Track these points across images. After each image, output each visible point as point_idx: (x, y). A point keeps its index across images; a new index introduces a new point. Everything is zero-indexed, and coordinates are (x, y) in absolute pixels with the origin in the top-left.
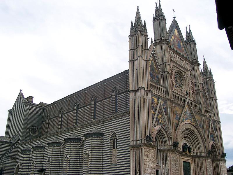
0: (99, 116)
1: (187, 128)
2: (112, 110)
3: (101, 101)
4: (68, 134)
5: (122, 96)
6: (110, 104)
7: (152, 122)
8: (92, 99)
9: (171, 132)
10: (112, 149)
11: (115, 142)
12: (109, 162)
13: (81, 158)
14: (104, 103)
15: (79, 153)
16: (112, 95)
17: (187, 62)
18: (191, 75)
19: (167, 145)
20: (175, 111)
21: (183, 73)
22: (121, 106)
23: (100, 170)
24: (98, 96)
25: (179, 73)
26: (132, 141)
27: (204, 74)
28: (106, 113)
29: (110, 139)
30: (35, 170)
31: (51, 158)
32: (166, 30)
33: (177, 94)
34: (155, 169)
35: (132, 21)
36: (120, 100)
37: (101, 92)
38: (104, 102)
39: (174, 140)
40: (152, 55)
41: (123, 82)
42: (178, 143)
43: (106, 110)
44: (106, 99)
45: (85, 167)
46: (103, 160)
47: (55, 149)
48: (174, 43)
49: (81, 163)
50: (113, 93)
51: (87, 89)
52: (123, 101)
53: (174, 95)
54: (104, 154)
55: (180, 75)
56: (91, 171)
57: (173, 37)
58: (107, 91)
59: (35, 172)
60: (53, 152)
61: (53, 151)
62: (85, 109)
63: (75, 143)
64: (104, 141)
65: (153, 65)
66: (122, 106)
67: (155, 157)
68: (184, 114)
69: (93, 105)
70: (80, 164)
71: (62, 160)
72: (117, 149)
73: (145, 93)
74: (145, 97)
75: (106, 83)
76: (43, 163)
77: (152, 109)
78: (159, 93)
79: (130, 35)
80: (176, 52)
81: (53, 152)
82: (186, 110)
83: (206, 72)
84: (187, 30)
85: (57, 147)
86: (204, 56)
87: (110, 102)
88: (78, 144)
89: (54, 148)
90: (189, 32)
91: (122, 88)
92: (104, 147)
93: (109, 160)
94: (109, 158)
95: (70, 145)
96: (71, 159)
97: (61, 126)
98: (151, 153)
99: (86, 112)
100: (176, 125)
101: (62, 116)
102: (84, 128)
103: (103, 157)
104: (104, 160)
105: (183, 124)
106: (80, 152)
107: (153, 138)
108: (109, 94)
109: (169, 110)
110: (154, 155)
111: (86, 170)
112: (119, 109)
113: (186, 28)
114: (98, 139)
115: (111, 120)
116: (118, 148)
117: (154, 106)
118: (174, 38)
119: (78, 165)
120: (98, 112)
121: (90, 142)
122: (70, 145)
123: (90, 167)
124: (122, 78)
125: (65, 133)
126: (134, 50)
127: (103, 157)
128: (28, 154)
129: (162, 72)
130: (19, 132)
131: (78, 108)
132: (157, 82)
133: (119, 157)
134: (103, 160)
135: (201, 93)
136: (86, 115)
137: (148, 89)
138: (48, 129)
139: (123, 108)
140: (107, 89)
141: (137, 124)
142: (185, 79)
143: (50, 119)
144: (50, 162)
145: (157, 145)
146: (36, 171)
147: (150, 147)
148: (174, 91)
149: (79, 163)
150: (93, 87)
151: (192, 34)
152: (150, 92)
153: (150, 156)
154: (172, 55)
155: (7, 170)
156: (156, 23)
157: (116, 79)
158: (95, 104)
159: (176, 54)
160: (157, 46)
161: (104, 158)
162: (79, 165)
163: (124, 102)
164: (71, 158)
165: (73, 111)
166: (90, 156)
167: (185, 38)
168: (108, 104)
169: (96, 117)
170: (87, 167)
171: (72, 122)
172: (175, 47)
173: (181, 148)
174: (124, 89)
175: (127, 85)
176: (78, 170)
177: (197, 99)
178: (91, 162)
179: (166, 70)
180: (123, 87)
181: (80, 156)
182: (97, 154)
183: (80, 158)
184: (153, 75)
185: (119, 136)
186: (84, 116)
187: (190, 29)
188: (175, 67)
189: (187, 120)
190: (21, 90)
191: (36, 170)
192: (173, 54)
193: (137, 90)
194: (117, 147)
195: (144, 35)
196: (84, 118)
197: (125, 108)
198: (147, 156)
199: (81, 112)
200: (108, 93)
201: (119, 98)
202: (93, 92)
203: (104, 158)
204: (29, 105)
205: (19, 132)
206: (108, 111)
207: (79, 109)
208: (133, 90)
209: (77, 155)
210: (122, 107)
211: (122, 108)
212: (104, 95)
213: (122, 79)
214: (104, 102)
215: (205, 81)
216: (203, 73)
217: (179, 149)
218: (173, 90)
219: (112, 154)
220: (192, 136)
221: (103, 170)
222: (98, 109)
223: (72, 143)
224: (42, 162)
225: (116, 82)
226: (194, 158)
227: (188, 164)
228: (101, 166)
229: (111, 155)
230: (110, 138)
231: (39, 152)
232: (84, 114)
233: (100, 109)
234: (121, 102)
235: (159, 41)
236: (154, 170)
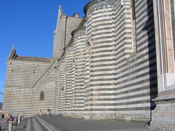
63: (83, 37)
96: (79, 63)
114: (105, 10)
164: (78, 62)
223: (79, 38)
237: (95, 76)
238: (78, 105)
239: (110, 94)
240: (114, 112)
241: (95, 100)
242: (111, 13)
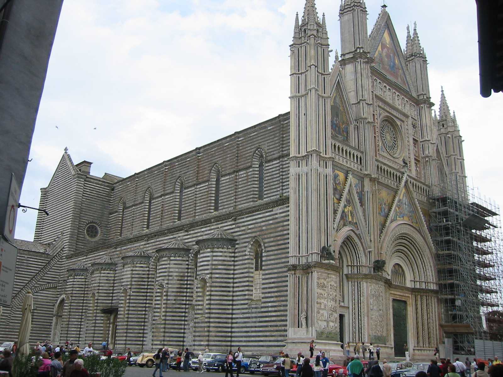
0: (225, 203)
1: (401, 234)
2: (252, 193)
3: (229, 174)
5: (273, 165)
6: (249, 180)
7: (334, 221)
8: (212, 169)
9: (371, 241)
10: (252, 270)
11: (258, 256)
12: (247, 297)
13: (189, 288)
14: (236, 179)
15: (186, 278)
16: (254, 163)
17: (406, 99)
18: (414, 126)
19: (362, 266)
20: (379, 199)
21: (399, 123)
22: (270, 186)
23: (227, 312)
24: (225, 165)
25: (389, 122)
26: (292, 257)
27: (441, 123)
28: (239, 200)
29: (249, 252)
30: (97, 310)
31: (129, 287)
32: (367, 33)
33: (385, 164)
34: (336, 313)
35: (297, 15)
36: (268, 175)
37: (230, 157)
38: (236, 176)
39: (377, 256)
40: (336, 86)
41: (276, 138)
42: (384, 263)
43: (239, 193)
44: (240, 170)
45: (199, 305)
46: (233, 292)
47: (137, 269)
48: (382, 59)
49: (189, 296)
50: (254, 160)
51: (201, 150)
52: (275, 176)
53: (378, 167)
54: (235, 281)
55: (392, 125)
56: (210, 313)
57: (380, 48)
58: (242, 154)
59: (97, 313)
60: (134, 274)
61: (134, 272)
62: (198, 190)
63: (178, 258)
64: (237, 255)
65: (338, 107)
66: (272, 186)
67: (338, 288)
68: (397, 206)
69: (213, 181)
70: (188, 298)
71: (151, 291)
72: (264, 272)
73: (322, 162)
74: (321, 170)
77: (334, 194)
78: (349, 163)
79: (292, 43)
80: (384, 79)
81: (134, 274)
82: (401, 197)
83: (446, 120)
84: (409, 33)
85: (142, 265)
86: (442, 87)
87: (250, 177)
88: (184, 261)
89: (136, 267)
90: (412, 36)
91: (273, 150)
92: (236, 268)
93: (247, 293)
94: (247, 288)
95: (168, 262)
96: (170, 290)
97: (148, 223)
98: (330, 282)
99: (200, 195)
100: (380, 226)
101: (150, 202)
102: (197, 229)
103: (233, 287)
104: (236, 291)
105: (394, 224)
106: (188, 276)
107: (334, 251)
108: (246, 162)
109: (368, 196)
110: (335, 285)
111: (200, 312)
112: (265, 191)
113: (408, 28)
114: (226, 250)
115: (251, 213)
116: (264, 270)
117: (339, 188)
118: (382, 49)
119: (183, 300)
120: (225, 197)
121: (208, 256)
122: (168, 262)
123: (207, 307)
124: (275, 130)
126: (300, 76)
127: (233, 287)
128: (83, 277)
129: (356, 120)
130: (62, 233)
131: (182, 187)
132: (346, 140)
133: (266, 288)
134: (233, 292)
135: (434, 163)
136: (199, 201)
137: (326, 154)
138: (122, 228)
139: (275, 190)
140: (242, 151)
141: (304, 224)
142: (401, 134)
143: (125, 208)
144: (128, 294)
145: (341, 266)
146: (98, 311)
147: (328, 270)
148: (378, 157)
149: (186, 296)
150: (214, 147)
151: (419, 40)
152: (330, 160)
153: (328, 287)
154: (376, 85)
155: (40, 309)
156: (346, 17)
157: (261, 131)
158: (218, 181)
159: (384, 82)
160: (347, 66)
161: (235, 289)
162: (186, 300)
163: (278, 179)
165: (172, 192)
166: (208, 284)
167: (405, 49)
168: (245, 182)
169: (220, 206)
170: (202, 305)
171: (170, 215)
172: (384, 68)
173: (390, 273)
174: (277, 151)
175: (284, 142)
176: (184, 310)
177: (425, 176)
178: (211, 295)
179: (364, 117)
180: (276, 149)
181: (187, 284)
182: (222, 280)
183: (187, 288)
184: (336, 125)
185: (266, 245)
186: (196, 204)
187: (415, 30)
188: (383, 109)
189: (403, 217)
190: (66, 149)
191: (98, 310)
192: (380, 82)
193: (303, 157)
194: (263, 268)
195: (321, 45)
196: (195, 207)
197: (279, 189)
198: (323, 286)
199: (190, 195)
200: (245, 159)
201: (267, 170)
202: (214, 155)
203: (235, 289)
204: (82, 178)
205: (62, 233)
206: (244, 195)
207: (186, 188)
208: (298, 155)
209: (182, 282)
210: (273, 187)
211: (272, 189)
212: (237, 163)
213: (274, 131)
214: (236, 176)
215: (443, 138)
216: (439, 123)
217: (385, 275)
218: (376, 156)
219: (252, 282)
220: (410, 247)
221: (234, 312)
222: (224, 191)
223: (172, 258)
224: (111, 295)
225: (262, 137)
226: (414, 293)
227: (403, 304)
228: (229, 305)
229: (250, 284)
230: (249, 250)
231: (104, 273)
232: (196, 200)
233: (228, 190)
234: (270, 178)
235: (351, 56)
236: (337, 316)
237: (212, 313)
238: (168, 339)
239: (226, 332)
240: (229, 348)
241: (212, 336)
242: (231, 255)
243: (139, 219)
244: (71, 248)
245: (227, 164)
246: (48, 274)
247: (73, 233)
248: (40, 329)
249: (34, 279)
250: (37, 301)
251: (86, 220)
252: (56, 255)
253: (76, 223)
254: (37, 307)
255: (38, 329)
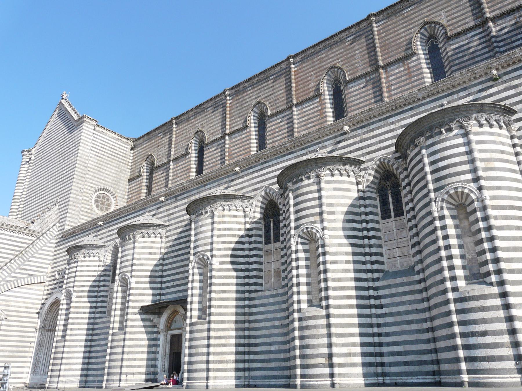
4: (283, 159)
13: (374, 237)
71: (257, 259)
75: (383, 22)
76: (161, 283)
89: (224, 216)
125: (266, 162)
224: (159, 279)
243: (182, 177)
244: (72, 222)
245: (356, 63)
246: (30, 261)
247: (75, 200)
248: (11, 354)
249: (5, 268)
250: (9, 306)
251: (95, 184)
252: (45, 233)
253: (79, 186)
254: (7, 315)
255: (7, 354)
